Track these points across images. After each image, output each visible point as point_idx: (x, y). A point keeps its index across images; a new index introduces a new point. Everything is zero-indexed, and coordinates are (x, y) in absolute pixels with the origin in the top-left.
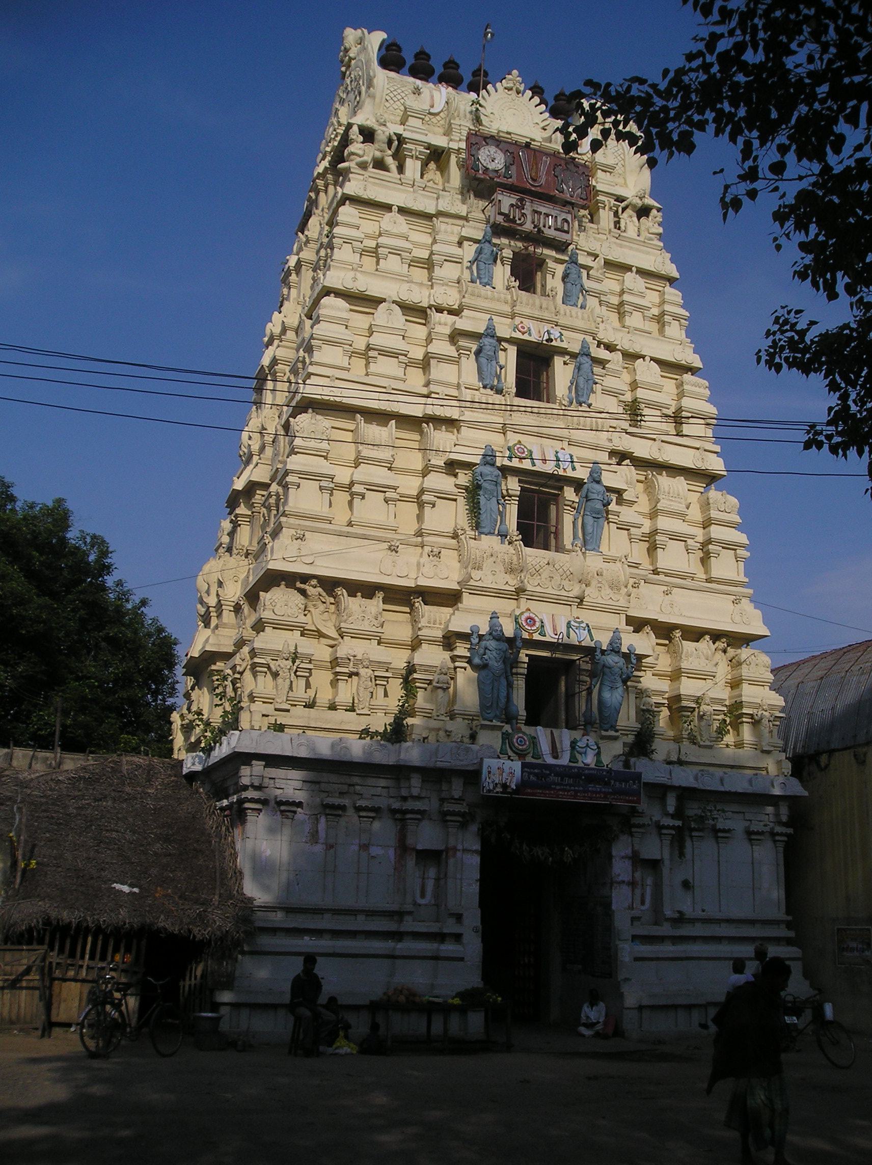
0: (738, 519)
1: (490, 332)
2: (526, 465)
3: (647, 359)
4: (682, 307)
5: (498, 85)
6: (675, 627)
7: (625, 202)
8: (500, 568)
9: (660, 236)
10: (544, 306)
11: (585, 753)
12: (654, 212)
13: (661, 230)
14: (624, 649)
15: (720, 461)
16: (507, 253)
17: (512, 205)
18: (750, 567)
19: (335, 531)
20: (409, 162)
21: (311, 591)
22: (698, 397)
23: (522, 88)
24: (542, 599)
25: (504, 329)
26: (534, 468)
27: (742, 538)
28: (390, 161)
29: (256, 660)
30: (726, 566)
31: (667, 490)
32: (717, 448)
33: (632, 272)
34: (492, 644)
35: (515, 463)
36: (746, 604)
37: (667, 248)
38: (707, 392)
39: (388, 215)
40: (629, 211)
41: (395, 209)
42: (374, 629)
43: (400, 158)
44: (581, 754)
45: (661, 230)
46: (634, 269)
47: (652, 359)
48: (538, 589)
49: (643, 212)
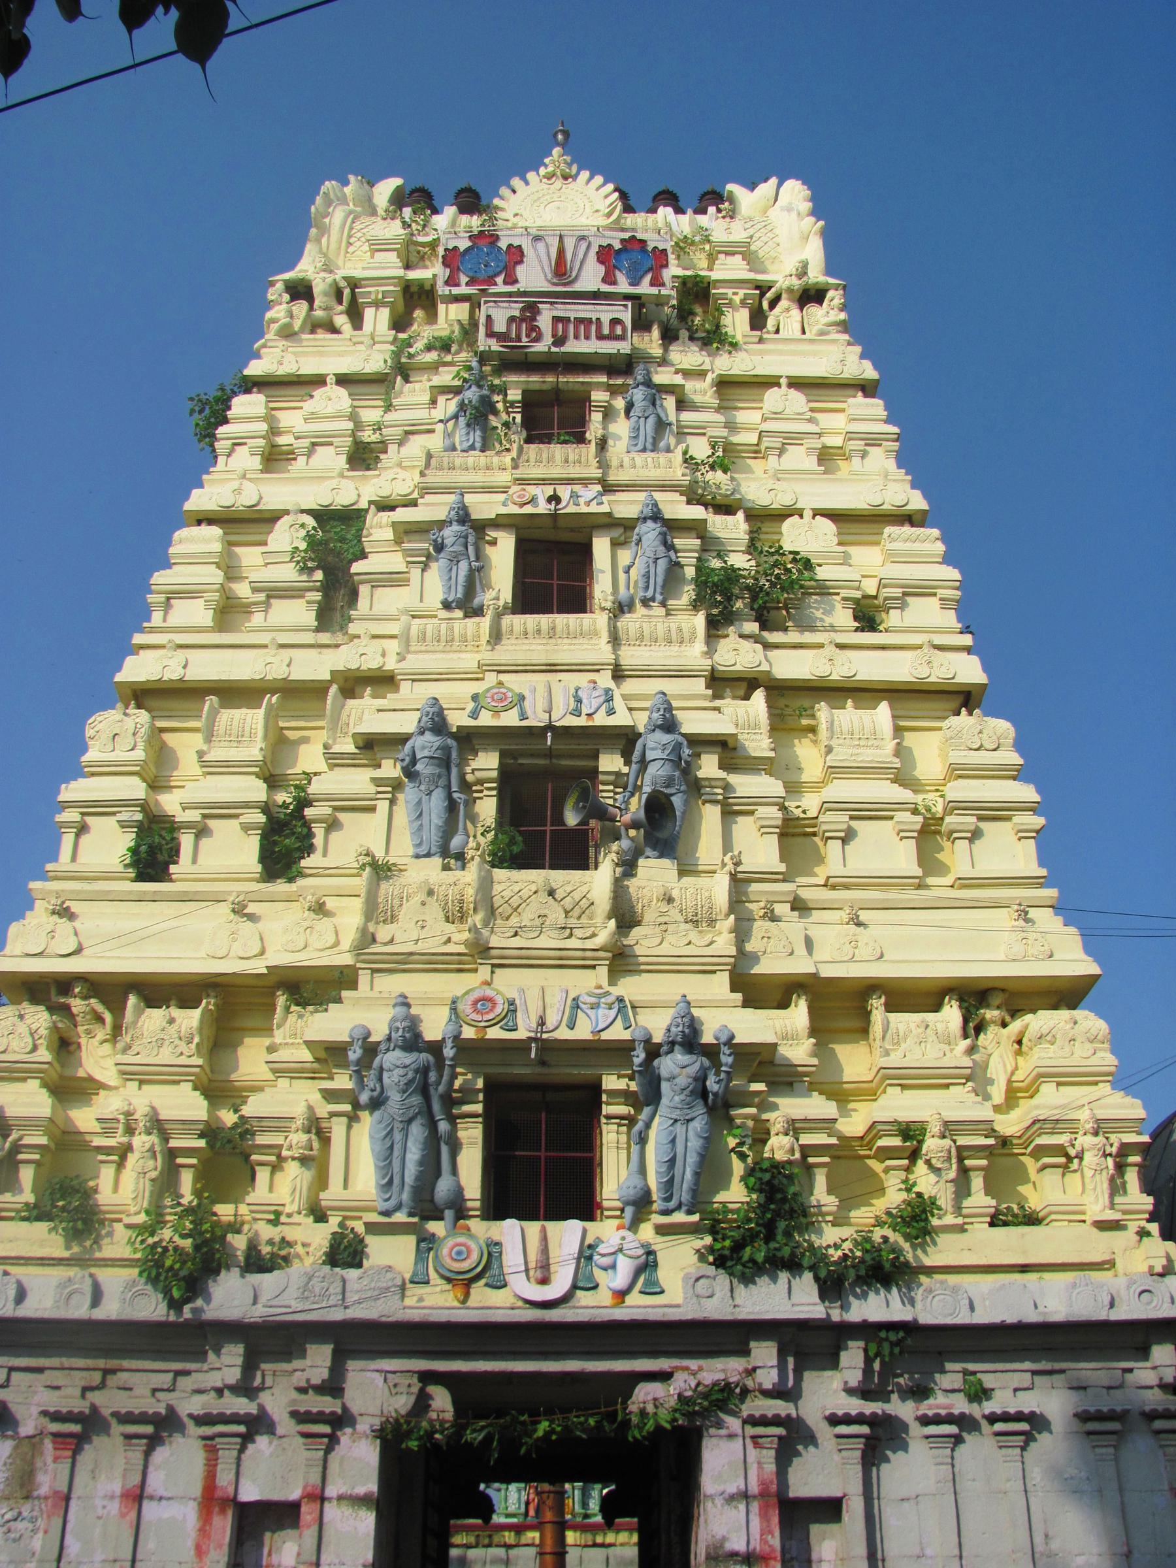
0: (1015, 759)
1: (463, 516)
2: (510, 719)
3: (808, 514)
4: (886, 422)
5: (531, 176)
6: (870, 988)
7: (773, 290)
8: (434, 913)
9: (844, 327)
10: (571, 458)
11: (613, 1267)
12: (830, 294)
13: (843, 316)
14: (707, 1038)
15: (975, 661)
16: (514, 395)
17: (512, 319)
18: (1046, 843)
19: (130, 892)
20: (369, 313)
21: (77, 1005)
22: (919, 556)
23: (574, 169)
24: (527, 961)
25: (484, 507)
26: (525, 723)
27: (1027, 793)
28: (341, 321)
29: (173, 1143)
30: (1009, 852)
31: (845, 729)
32: (967, 640)
33: (778, 385)
34: (393, 1058)
35: (486, 719)
36: (1045, 919)
37: (856, 340)
38: (940, 547)
39: (318, 393)
40: (784, 303)
41: (331, 380)
42: (183, 1060)
43: (355, 315)
44: (605, 1269)
45: (843, 316)
46: (783, 381)
47: (817, 513)
48: (517, 942)
49: (811, 296)
